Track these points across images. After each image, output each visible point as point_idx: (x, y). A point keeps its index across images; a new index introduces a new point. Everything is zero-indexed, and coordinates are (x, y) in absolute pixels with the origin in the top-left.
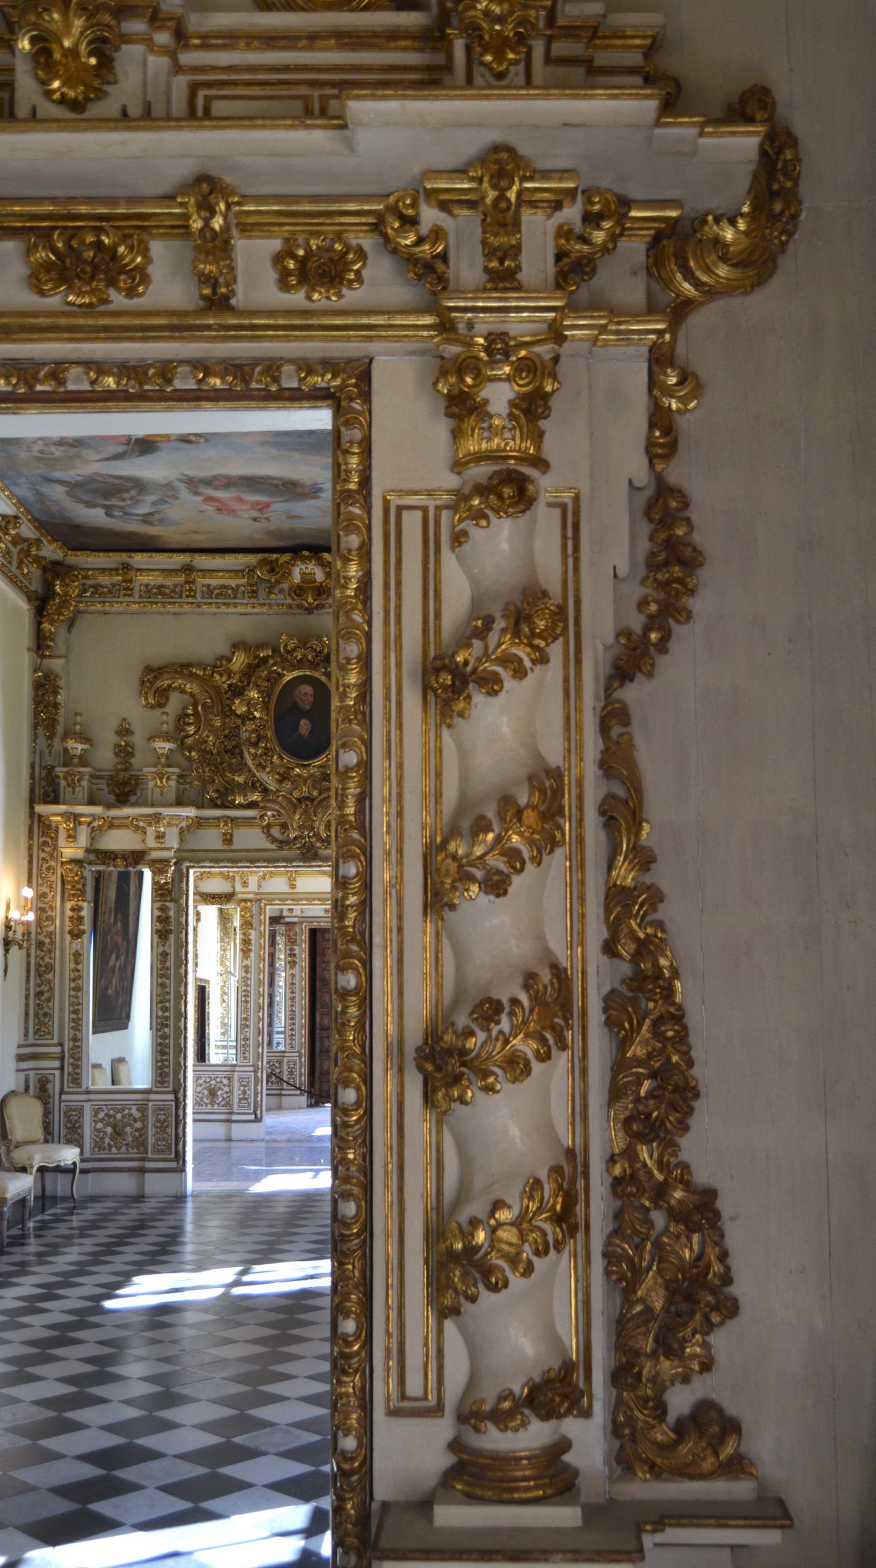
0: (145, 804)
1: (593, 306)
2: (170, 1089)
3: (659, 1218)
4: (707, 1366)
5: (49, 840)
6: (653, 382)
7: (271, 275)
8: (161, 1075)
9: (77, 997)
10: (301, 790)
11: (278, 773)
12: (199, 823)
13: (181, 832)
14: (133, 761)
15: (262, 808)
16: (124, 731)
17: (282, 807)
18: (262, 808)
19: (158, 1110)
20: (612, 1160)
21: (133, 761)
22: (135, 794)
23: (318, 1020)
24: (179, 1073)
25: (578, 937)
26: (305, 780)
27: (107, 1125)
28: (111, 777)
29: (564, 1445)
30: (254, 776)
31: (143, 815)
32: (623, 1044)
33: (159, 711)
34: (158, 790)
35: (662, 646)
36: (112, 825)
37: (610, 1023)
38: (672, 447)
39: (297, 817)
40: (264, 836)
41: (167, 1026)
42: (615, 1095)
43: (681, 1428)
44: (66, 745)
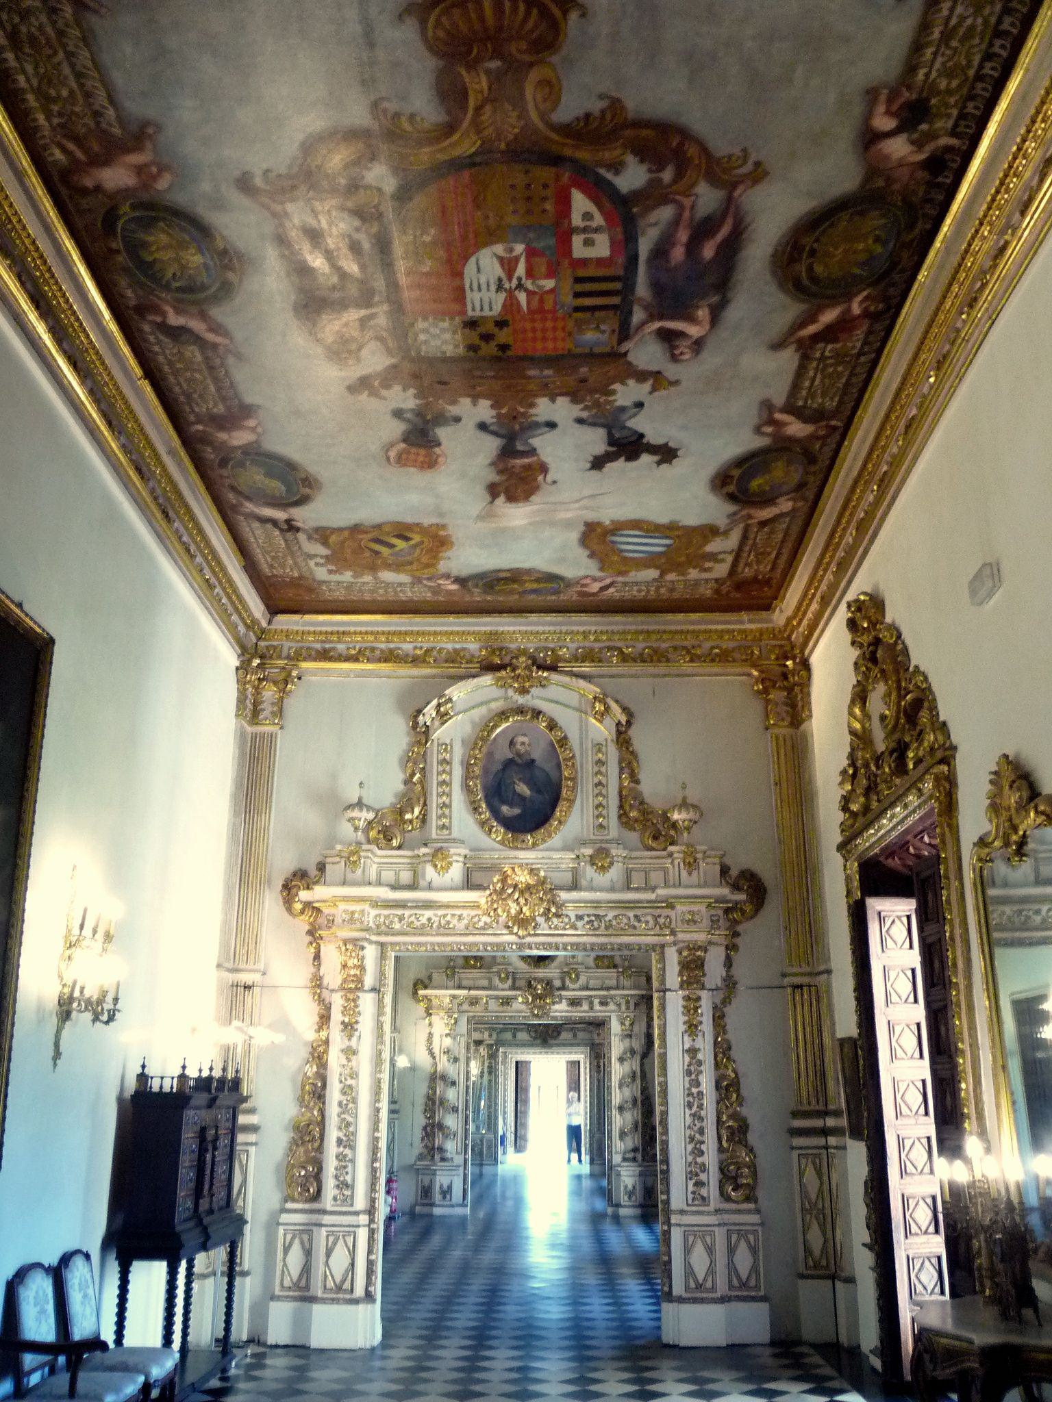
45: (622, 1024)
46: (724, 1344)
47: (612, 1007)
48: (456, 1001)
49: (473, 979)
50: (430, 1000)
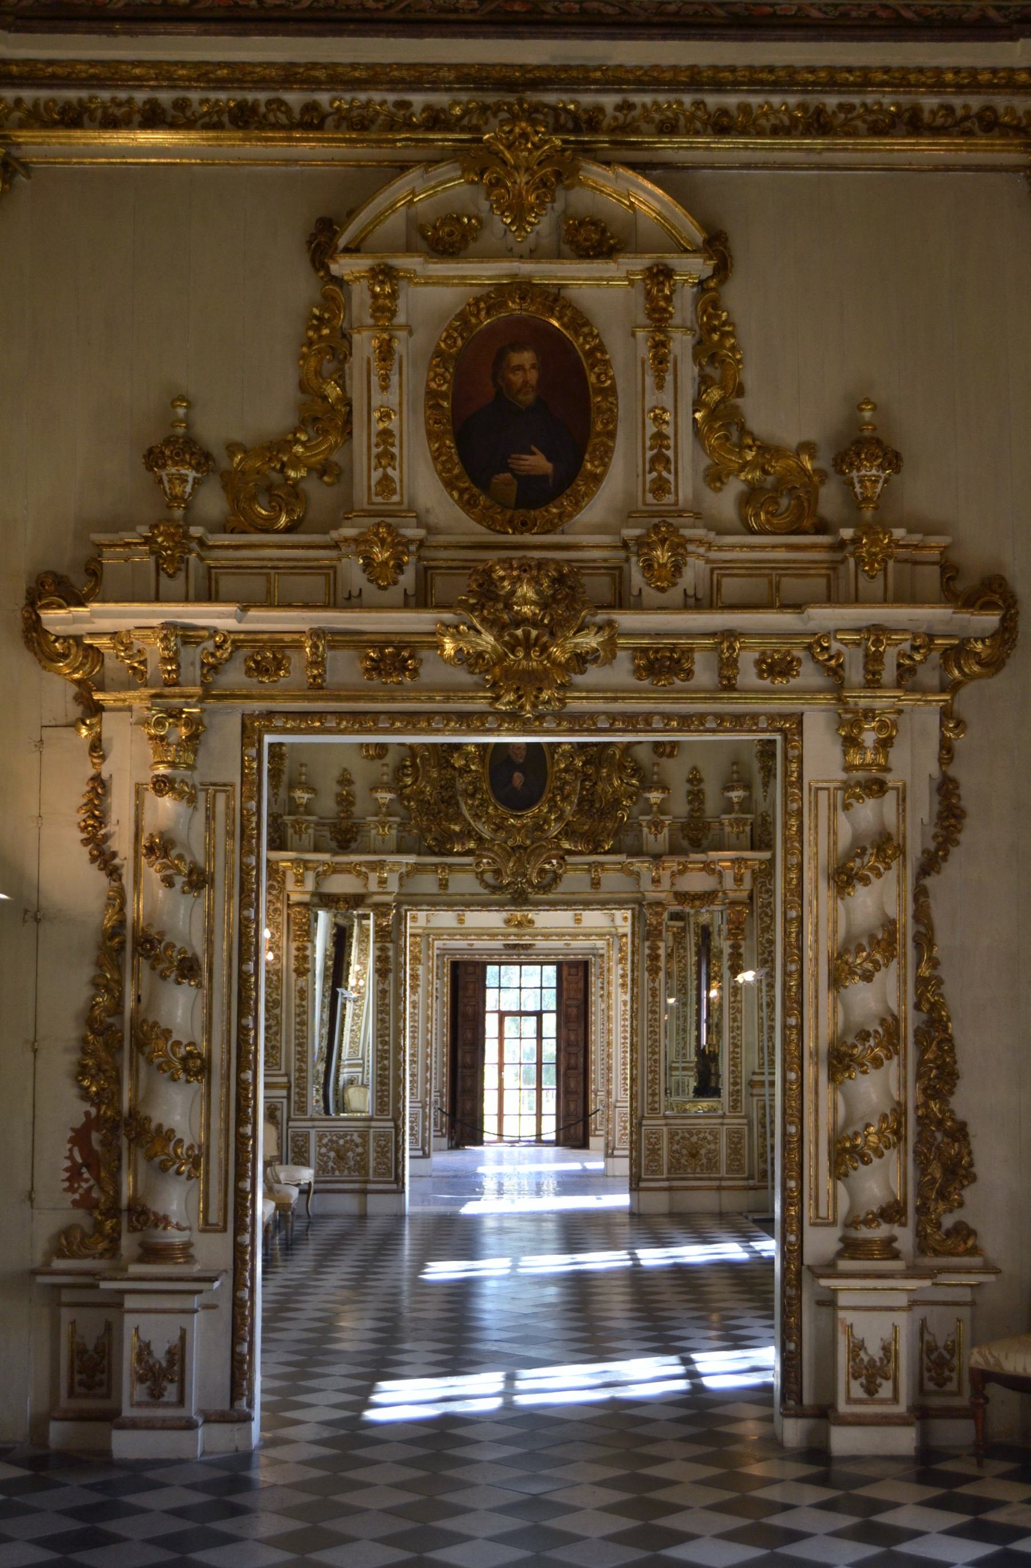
0: (369, 853)
1: (913, 690)
2: (390, 1117)
3: (939, 1136)
4: (961, 1204)
5: (275, 884)
6: (942, 724)
7: (754, 671)
8: (381, 1104)
9: (301, 1031)
10: (515, 839)
11: (494, 824)
12: (418, 869)
13: (401, 878)
14: (353, 809)
15: (478, 855)
16: (345, 780)
17: (497, 854)
18: (478, 855)
19: (379, 1136)
20: (917, 1108)
21: (353, 809)
22: (356, 841)
23: (460, 1058)
24: (398, 1102)
25: (902, 999)
26: (519, 830)
27: (331, 1149)
28: (334, 825)
29: (893, 1239)
30: (470, 824)
31: (366, 862)
32: (923, 1052)
33: (378, 763)
34: (380, 837)
35: (945, 858)
36: (336, 869)
37: (917, 1043)
38: (951, 759)
39: (511, 864)
40: (478, 882)
41: (387, 1058)
42: (919, 1077)
43: (948, 1234)
44: (292, 794)
45: (851, 742)
47: (808, 675)
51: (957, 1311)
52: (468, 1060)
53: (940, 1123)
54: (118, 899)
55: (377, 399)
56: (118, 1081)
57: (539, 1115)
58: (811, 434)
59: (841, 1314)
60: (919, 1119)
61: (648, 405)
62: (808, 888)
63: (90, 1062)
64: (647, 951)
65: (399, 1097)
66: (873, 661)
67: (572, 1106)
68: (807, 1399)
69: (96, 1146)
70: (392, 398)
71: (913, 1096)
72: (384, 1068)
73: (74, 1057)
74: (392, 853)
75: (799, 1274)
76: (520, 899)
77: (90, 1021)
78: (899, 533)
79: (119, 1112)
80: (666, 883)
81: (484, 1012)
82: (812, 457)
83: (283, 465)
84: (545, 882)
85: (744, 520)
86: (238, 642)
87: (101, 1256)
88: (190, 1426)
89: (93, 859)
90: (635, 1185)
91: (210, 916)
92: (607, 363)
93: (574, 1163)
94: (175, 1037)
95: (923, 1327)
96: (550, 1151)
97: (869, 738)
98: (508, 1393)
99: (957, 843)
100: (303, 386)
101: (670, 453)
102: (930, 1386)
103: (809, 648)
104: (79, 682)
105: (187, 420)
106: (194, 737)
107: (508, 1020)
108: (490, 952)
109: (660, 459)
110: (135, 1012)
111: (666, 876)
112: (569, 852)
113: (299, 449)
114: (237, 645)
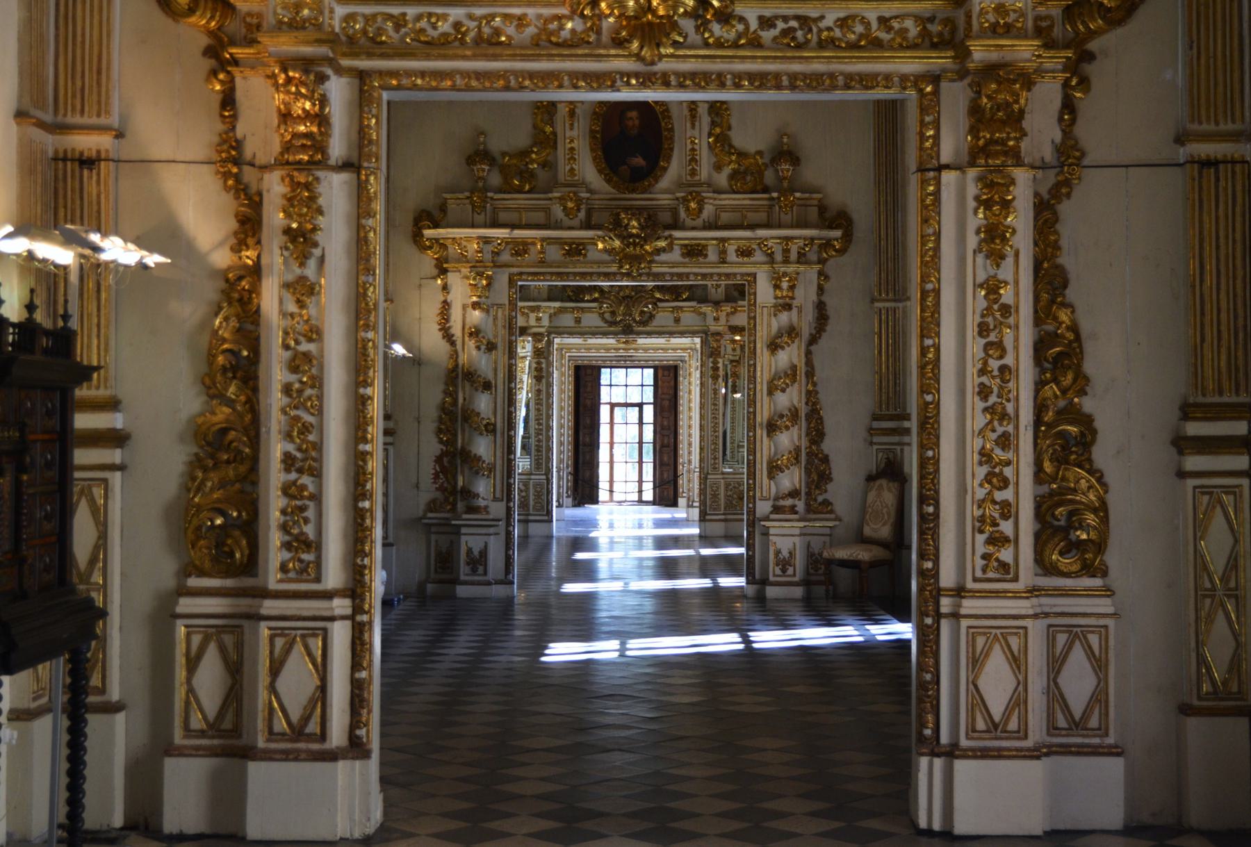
0: (529, 300)
1: (806, 263)
4: (826, 491)
7: (735, 254)
12: (561, 310)
25: (800, 401)
35: (820, 338)
37: (807, 420)
42: (807, 435)
43: (820, 504)
45: (777, 287)
46: (1038, 831)
47: (759, 256)
48: (490, 248)
49: (518, 210)
50: (444, 247)
51: (823, 538)
52: (587, 439)
53: (816, 455)
54: (455, 355)
55: (568, 134)
56: (455, 435)
57: (640, 481)
58: (761, 147)
59: (771, 538)
60: (807, 454)
61: (689, 134)
62: (758, 351)
63: (443, 427)
64: (711, 365)
65: (549, 459)
66: (786, 252)
67: (665, 476)
68: (757, 576)
69: (446, 464)
70: (575, 133)
71: (804, 443)
72: (539, 441)
73: (435, 425)
74: (545, 300)
75: (754, 521)
76: (628, 330)
77: (443, 408)
78: (798, 195)
79: (456, 449)
80: (723, 321)
81: (599, 404)
82: (761, 157)
83: (527, 163)
84: (644, 319)
85: (731, 186)
86: (507, 242)
87: (448, 512)
88: (489, 583)
89: (444, 337)
90: (703, 518)
91: (496, 363)
92: (670, 117)
93: (666, 513)
94: (482, 416)
95: (809, 546)
96: (650, 508)
97: (785, 285)
98: (622, 650)
99: (825, 331)
100: (535, 127)
101: (698, 158)
102: (812, 571)
103: (759, 244)
104: (437, 259)
105: (484, 143)
106: (489, 285)
107: (616, 409)
108: (604, 359)
109: (693, 160)
110: (463, 405)
111: (723, 315)
112: (660, 300)
113: (534, 156)
114: (507, 243)
